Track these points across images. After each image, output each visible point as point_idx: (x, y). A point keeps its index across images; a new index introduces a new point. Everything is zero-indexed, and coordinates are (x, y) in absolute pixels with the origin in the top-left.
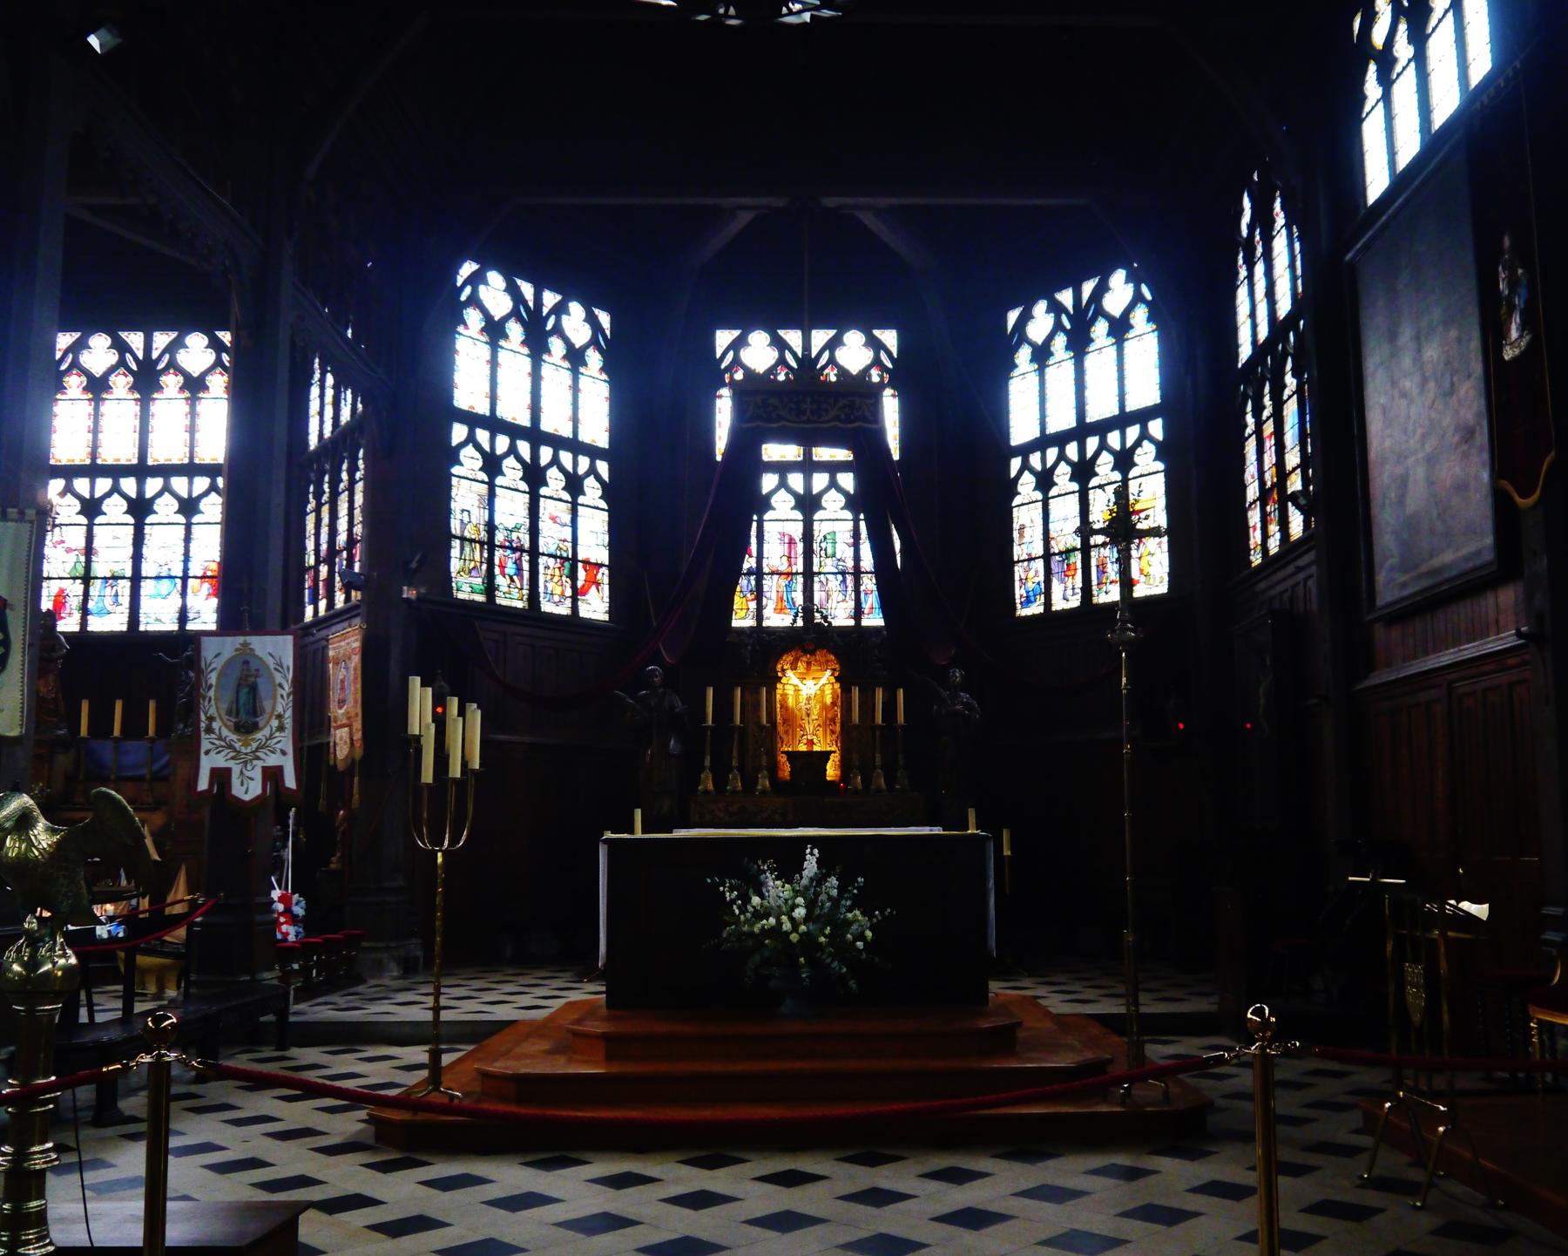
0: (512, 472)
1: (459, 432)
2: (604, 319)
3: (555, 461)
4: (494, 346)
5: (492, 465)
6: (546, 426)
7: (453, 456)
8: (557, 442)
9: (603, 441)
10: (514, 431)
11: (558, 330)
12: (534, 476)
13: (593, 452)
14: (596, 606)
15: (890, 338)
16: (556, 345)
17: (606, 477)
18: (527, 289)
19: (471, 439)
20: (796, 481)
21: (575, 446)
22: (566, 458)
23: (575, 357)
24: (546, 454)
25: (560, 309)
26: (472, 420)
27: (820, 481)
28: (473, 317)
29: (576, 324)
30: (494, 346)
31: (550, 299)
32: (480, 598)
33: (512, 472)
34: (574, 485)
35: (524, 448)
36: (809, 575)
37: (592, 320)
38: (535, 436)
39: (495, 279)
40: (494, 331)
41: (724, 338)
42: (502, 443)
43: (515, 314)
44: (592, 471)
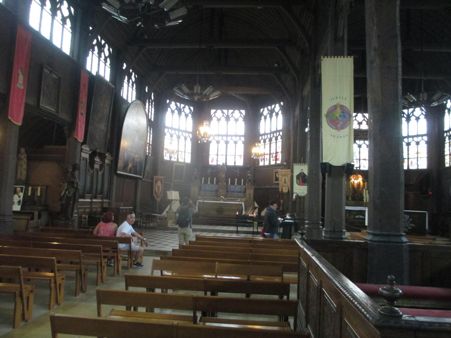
0: (175, 137)
1: (166, 130)
2: (192, 108)
3: (182, 134)
4: (173, 114)
5: (171, 136)
6: (181, 129)
7: (165, 134)
8: (183, 131)
9: (191, 131)
10: (175, 129)
11: (184, 111)
12: (179, 137)
13: (189, 133)
14: (188, 160)
15: (243, 112)
16: (183, 113)
17: (191, 137)
18: (178, 104)
19: (168, 131)
20: (225, 138)
21: (186, 132)
22: (184, 133)
23: (187, 116)
24: (181, 133)
25: (184, 107)
26: (168, 128)
27: (229, 138)
28: (169, 109)
29: (187, 109)
30: (173, 114)
31: (182, 105)
32: (169, 159)
33: (175, 137)
34: (186, 138)
35: (177, 132)
36: (226, 155)
37: (190, 109)
38: (179, 130)
39: (173, 103)
40: (173, 112)
41: (213, 111)
42: (173, 131)
43: (176, 109)
44: (189, 136)
